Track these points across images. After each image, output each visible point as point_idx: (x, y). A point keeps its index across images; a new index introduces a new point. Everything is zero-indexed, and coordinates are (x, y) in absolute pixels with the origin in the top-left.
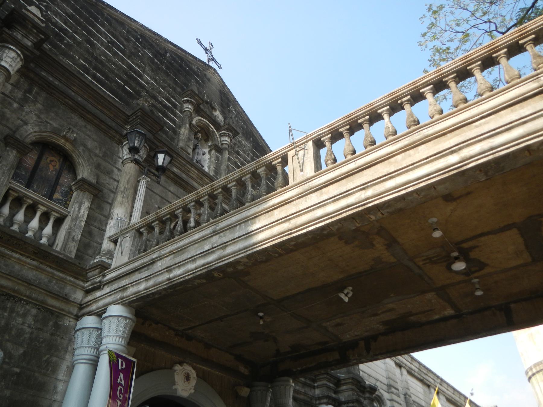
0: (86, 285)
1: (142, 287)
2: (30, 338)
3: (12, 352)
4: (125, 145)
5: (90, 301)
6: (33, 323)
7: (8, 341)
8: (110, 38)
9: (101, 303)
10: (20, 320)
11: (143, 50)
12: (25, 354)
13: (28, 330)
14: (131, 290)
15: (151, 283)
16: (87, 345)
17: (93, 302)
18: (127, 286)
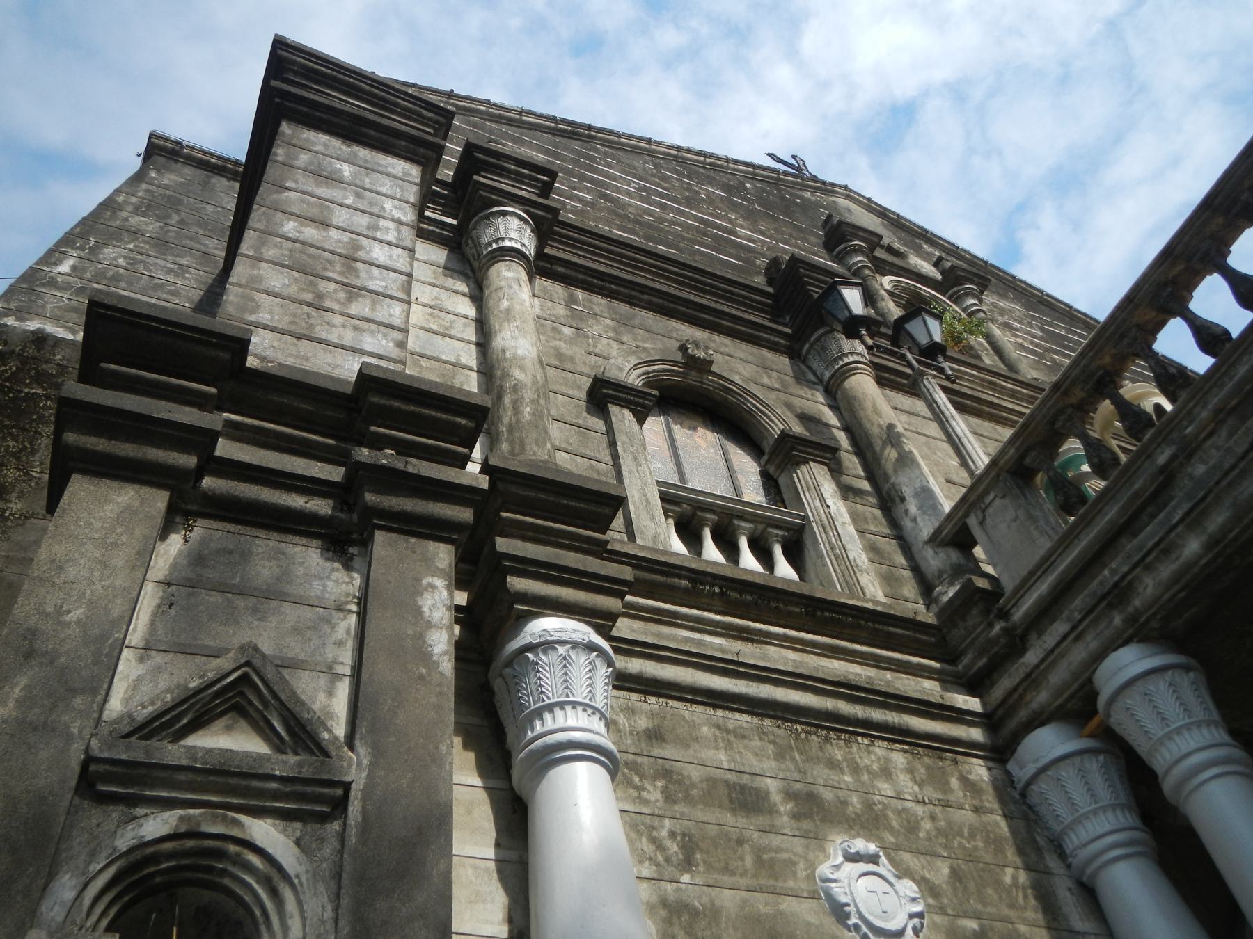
0: (960, 667)
1: (1193, 546)
2: (938, 830)
3: (928, 876)
4: (808, 352)
5: (1015, 689)
6: (916, 788)
7: (898, 847)
8: (635, 182)
9: (1058, 676)
10: (885, 788)
11: (702, 189)
12: (956, 874)
13: (919, 810)
14: (1149, 587)
15: (1217, 520)
16: (1093, 806)
17: (1025, 691)
18: (1129, 577)
